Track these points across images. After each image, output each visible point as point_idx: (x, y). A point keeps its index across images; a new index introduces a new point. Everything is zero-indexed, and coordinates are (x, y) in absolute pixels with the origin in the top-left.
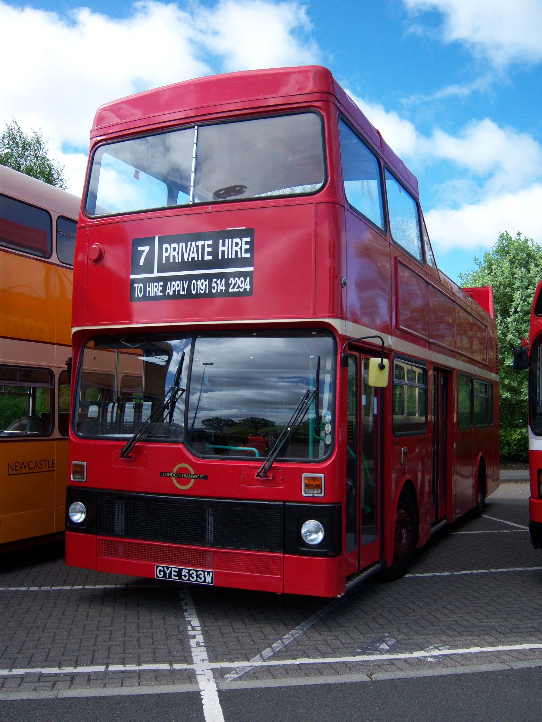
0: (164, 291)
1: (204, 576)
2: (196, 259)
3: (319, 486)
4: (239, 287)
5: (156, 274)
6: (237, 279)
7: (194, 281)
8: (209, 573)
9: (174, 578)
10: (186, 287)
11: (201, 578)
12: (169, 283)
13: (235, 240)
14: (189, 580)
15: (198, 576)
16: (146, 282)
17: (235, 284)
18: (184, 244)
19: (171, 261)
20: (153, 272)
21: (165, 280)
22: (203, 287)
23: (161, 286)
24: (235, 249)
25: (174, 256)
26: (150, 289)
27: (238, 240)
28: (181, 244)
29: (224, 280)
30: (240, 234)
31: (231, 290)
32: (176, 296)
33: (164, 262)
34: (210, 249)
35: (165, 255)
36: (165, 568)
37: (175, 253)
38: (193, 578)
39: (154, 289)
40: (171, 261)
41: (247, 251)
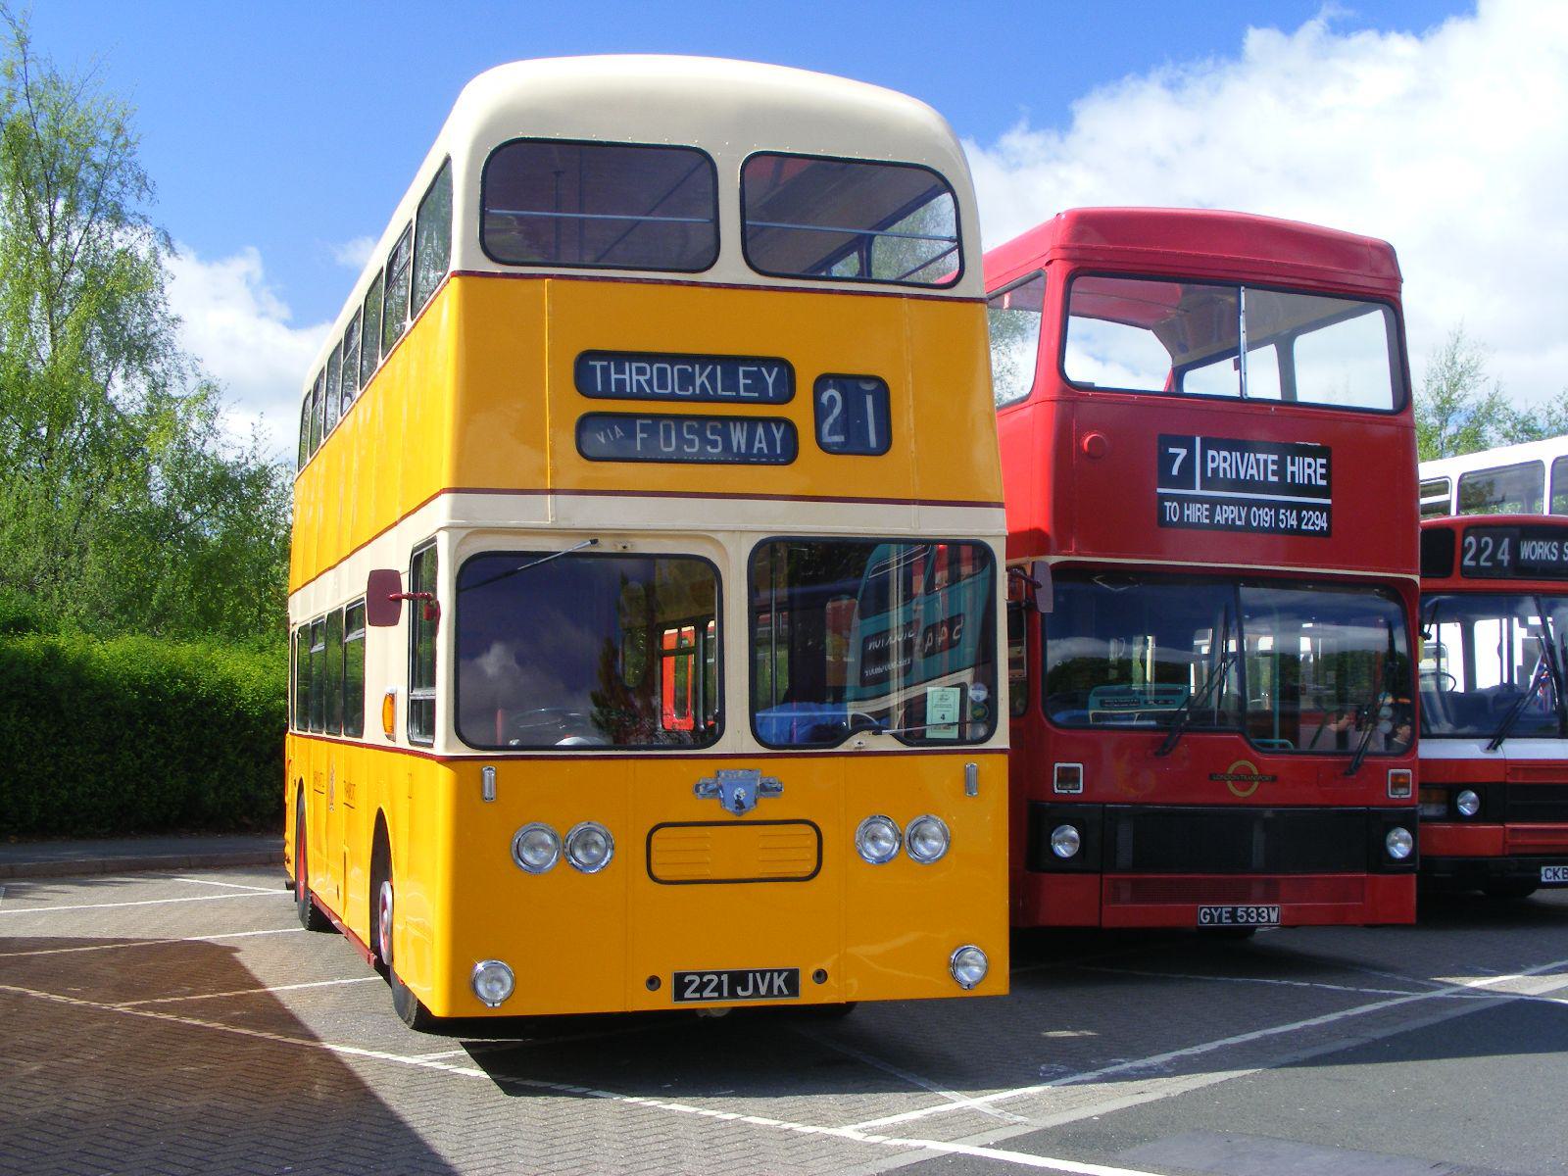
0: (1211, 517)
1: (1269, 916)
2: (1256, 478)
3: (1405, 785)
4: (1314, 524)
5: (1198, 491)
6: (1311, 513)
7: (1254, 509)
8: (1274, 909)
9: (1226, 922)
10: (1243, 515)
11: (1263, 918)
12: (1219, 507)
13: (1308, 460)
14: (1247, 921)
15: (1259, 915)
16: (1182, 500)
17: (1309, 519)
18: (1238, 454)
19: (1221, 475)
20: (1193, 487)
21: (1214, 503)
22: (1268, 519)
23: (1207, 510)
24: (1307, 471)
25: (1225, 469)
26: (1189, 512)
27: (1311, 460)
28: (1234, 453)
29: (1295, 512)
30: (1314, 453)
31: (1304, 527)
32: (1230, 527)
33: (1209, 475)
34: (1275, 467)
35: (1210, 465)
36: (1213, 910)
37: (1227, 465)
38: (1252, 918)
39: (1196, 513)
40: (1221, 475)
41: (1323, 477)
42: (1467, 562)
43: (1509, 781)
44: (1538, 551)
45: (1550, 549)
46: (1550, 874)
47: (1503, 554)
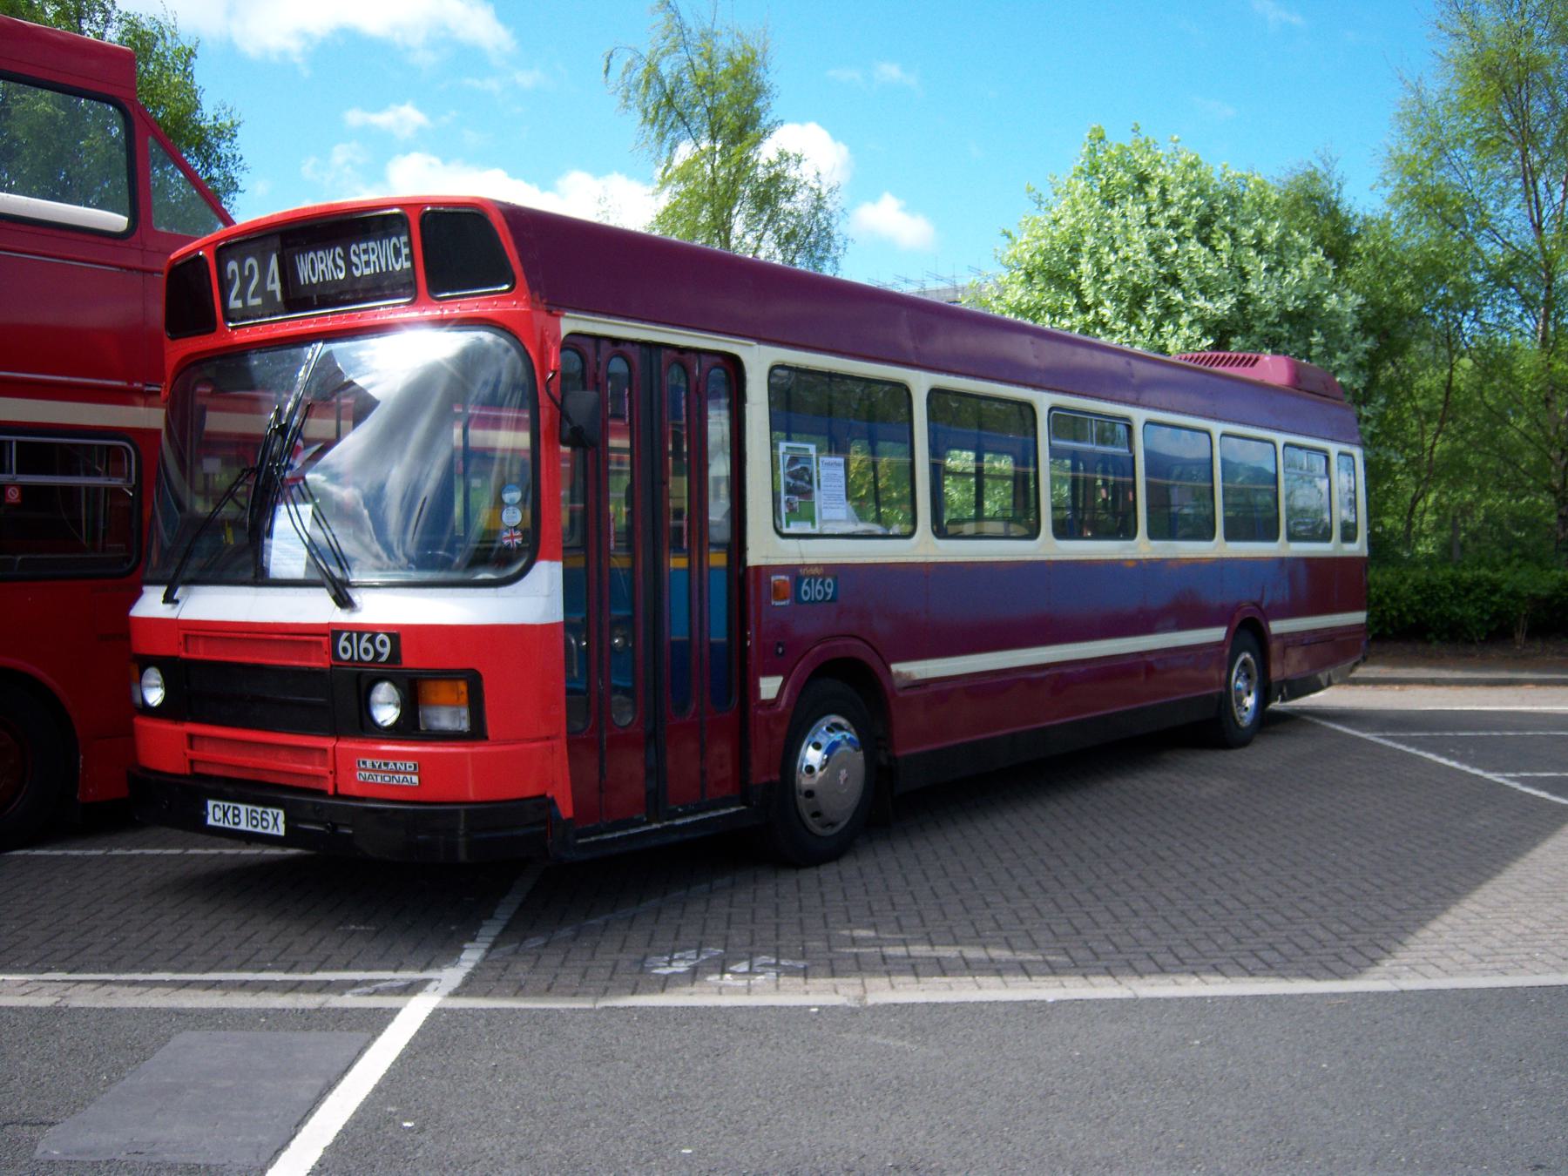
42: (235, 304)
43: (184, 655)
44: (320, 267)
45: (334, 260)
46: (219, 814)
47: (273, 281)
